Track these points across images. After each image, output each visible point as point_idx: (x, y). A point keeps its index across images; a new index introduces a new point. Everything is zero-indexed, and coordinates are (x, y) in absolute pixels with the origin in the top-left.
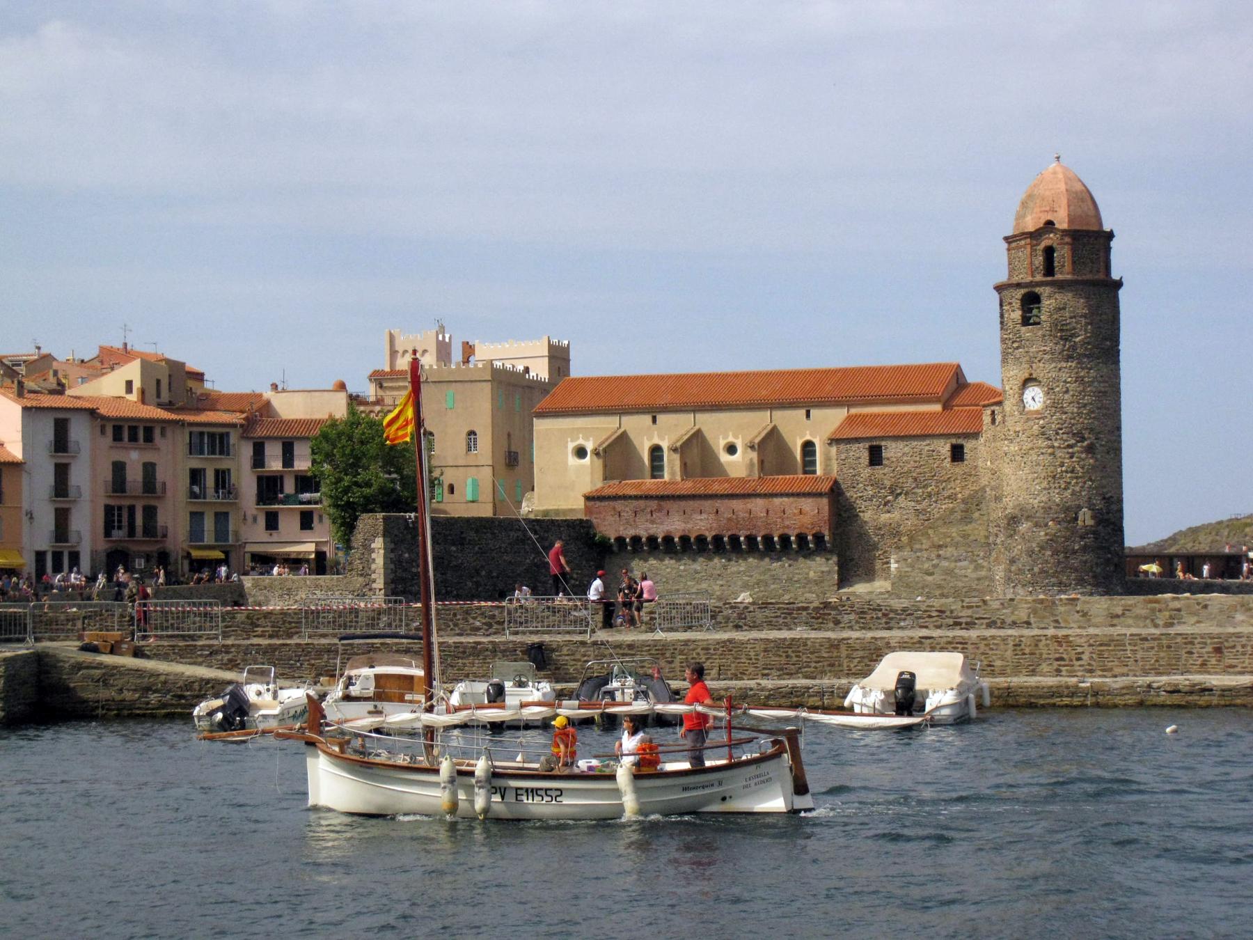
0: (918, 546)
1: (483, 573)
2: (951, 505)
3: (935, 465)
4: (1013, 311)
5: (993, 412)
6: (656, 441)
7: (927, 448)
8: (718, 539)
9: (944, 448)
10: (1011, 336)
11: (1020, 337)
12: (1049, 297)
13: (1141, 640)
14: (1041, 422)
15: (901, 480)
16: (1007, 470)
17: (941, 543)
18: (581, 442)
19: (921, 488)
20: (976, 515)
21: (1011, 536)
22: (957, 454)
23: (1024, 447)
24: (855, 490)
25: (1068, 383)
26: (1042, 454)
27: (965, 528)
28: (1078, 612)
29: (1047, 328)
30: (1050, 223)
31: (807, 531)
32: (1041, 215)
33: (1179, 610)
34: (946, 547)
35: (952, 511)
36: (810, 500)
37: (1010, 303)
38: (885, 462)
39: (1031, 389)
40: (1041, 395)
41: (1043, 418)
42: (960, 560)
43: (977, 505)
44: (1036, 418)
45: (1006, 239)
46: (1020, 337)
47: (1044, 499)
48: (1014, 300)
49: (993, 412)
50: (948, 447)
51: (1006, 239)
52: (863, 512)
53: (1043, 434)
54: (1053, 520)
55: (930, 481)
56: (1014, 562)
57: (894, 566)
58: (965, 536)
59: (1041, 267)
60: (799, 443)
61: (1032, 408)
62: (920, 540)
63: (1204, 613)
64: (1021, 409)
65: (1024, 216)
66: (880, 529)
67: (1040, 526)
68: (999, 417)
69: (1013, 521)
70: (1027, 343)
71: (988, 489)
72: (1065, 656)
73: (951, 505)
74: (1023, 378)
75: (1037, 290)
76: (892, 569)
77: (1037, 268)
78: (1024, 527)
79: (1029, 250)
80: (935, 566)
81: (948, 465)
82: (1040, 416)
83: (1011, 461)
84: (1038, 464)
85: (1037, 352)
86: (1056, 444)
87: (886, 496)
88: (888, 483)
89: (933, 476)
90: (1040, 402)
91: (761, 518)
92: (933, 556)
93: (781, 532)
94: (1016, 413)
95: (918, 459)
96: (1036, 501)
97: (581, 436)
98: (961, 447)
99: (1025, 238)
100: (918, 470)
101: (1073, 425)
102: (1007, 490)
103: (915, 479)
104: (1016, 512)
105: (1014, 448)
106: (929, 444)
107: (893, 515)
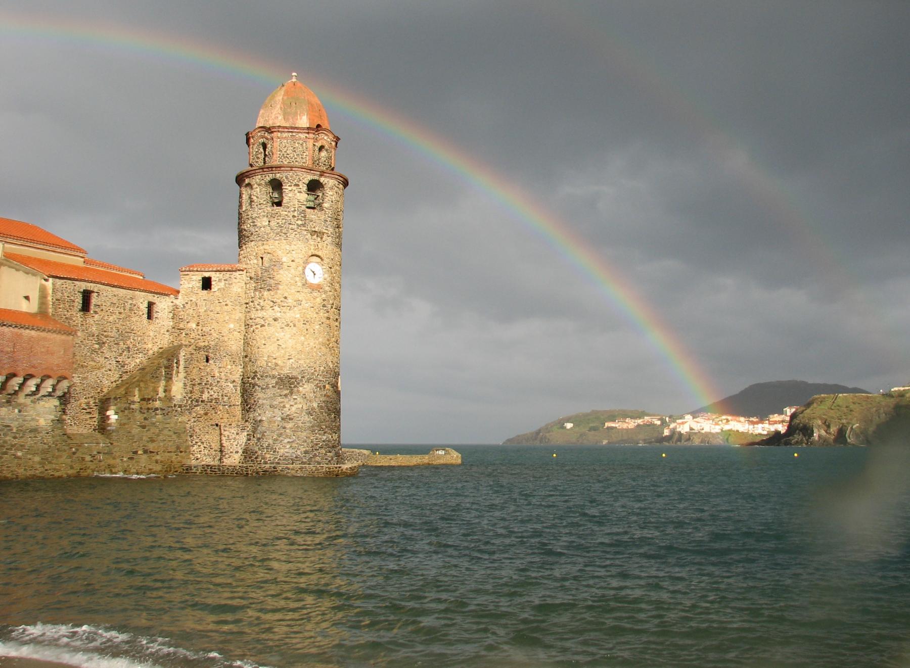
7: (130, 302)
9: (144, 307)
10: (296, 214)
12: (331, 188)
21: (286, 395)
29: (330, 215)
30: (319, 126)
37: (297, 185)
40: (321, 272)
46: (305, 217)
53: (324, 306)
54: (329, 384)
55: (130, 334)
57: (113, 416)
64: (304, 281)
68: (222, 284)
75: (322, 180)
79: (311, 143)
83: (288, 325)
89: (133, 330)
99: (308, 133)
104: (295, 374)
105: (295, 314)
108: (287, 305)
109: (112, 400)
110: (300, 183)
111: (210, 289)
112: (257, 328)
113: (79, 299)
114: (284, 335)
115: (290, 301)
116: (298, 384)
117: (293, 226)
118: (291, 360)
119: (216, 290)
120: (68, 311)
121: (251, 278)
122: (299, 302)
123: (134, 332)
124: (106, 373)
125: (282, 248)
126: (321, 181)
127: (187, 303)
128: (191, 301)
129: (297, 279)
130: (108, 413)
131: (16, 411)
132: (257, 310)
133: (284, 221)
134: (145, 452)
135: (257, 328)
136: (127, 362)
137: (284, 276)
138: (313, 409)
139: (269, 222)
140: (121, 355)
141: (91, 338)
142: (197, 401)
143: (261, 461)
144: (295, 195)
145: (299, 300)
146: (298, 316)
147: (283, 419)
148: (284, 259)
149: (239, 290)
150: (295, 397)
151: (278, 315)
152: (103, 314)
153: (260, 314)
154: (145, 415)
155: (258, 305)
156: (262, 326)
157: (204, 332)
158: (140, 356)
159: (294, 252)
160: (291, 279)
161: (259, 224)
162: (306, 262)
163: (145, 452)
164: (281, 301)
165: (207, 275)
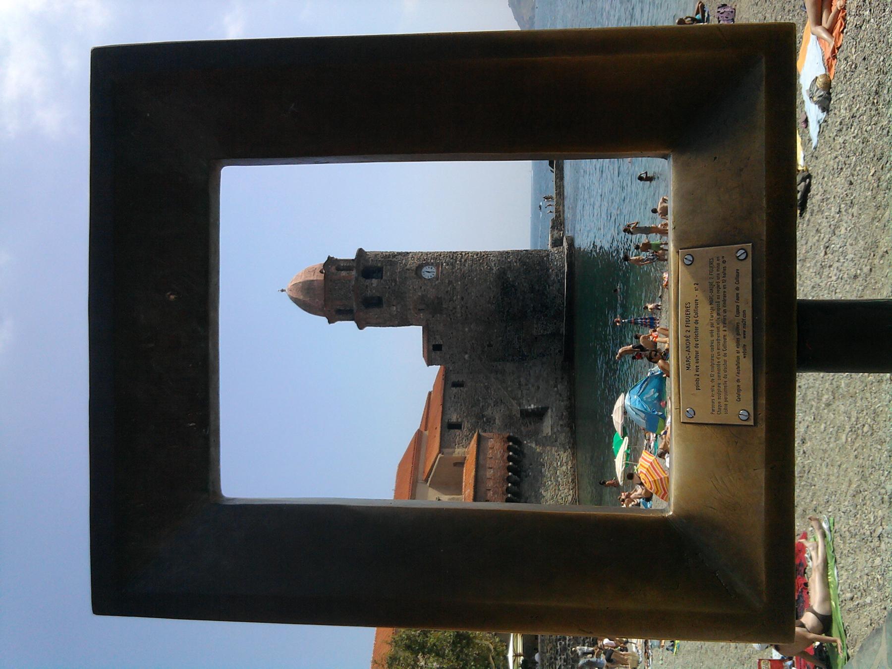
0: (519, 396)
3: (465, 395)
4: (372, 284)
7: (452, 399)
9: (455, 390)
10: (387, 287)
15: (473, 414)
19: (479, 404)
20: (500, 367)
21: (516, 290)
22: (456, 385)
23: (459, 275)
30: (321, 272)
31: (506, 445)
32: (315, 276)
34: (520, 381)
38: (460, 420)
39: (423, 274)
40: (427, 267)
41: (442, 264)
42: (530, 374)
44: (442, 267)
50: (454, 388)
56: (532, 287)
57: (532, 406)
59: (348, 272)
61: (435, 274)
66: (506, 425)
68: (437, 337)
70: (394, 276)
74: (415, 276)
76: (535, 407)
80: (533, 386)
81: (466, 389)
82: (440, 267)
83: (466, 290)
84: (472, 266)
85: (400, 266)
86: (460, 258)
90: (431, 268)
91: (494, 473)
93: (506, 461)
94: (437, 282)
95: (459, 404)
96: (494, 268)
100: (467, 404)
103: (472, 407)
106: (451, 398)
107: (497, 418)
108: (452, 292)
109: (522, 408)
111: (441, 345)
112: (469, 312)
113: (452, 431)
114: (473, 292)
115: (449, 289)
116: (507, 282)
118: (491, 287)
119: (441, 341)
120: (463, 438)
121: (433, 317)
122: (450, 283)
123: (473, 396)
125: (411, 295)
126: (362, 269)
127: (451, 361)
128: (449, 358)
129: (434, 284)
130: (530, 411)
131: (531, 466)
132: (456, 312)
133: (393, 295)
134: (556, 386)
135: (469, 312)
137: (432, 294)
139: (394, 306)
140: (489, 405)
141: (480, 424)
142: (519, 352)
143: (562, 307)
144: (374, 287)
145: (449, 283)
146: (459, 283)
147: (532, 293)
148: (420, 294)
149: (442, 325)
150: (517, 284)
151: (459, 297)
153: (458, 309)
154: (530, 386)
155: (452, 311)
156: (467, 307)
157: (471, 348)
158: (490, 391)
159: (415, 287)
160: (433, 288)
161: (395, 313)
162: (421, 277)
163: (556, 386)
164: (450, 295)
165: (431, 348)
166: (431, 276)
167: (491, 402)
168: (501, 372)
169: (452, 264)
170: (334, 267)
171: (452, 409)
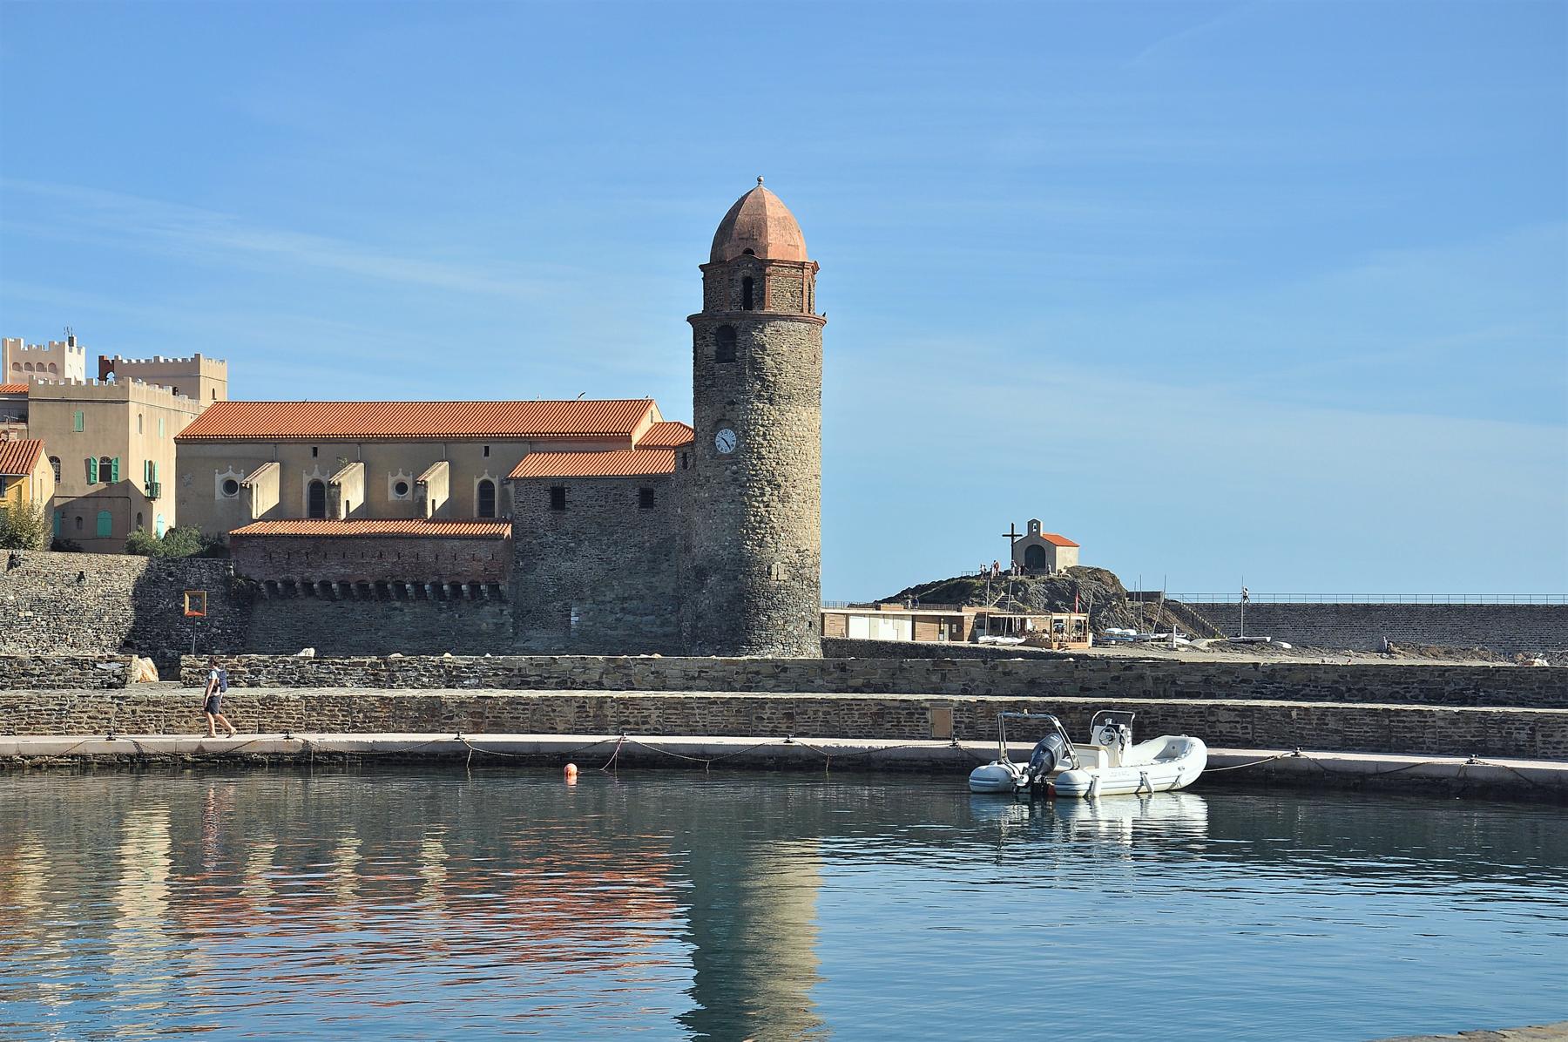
1: (106, 619)
2: (638, 554)
5: (685, 454)
6: (316, 475)
7: (614, 491)
8: (381, 585)
9: (633, 494)
11: (713, 375)
13: (710, 703)
14: (735, 468)
16: (697, 519)
17: (626, 595)
18: (231, 475)
20: (665, 565)
24: (535, 535)
25: (762, 426)
26: (733, 501)
27: (654, 580)
28: (652, 673)
31: (480, 580)
33: (757, 673)
34: (631, 600)
35: (639, 561)
36: (484, 544)
38: (567, 506)
42: (646, 615)
43: (665, 555)
45: (702, 267)
46: (713, 375)
47: (735, 551)
48: (707, 335)
49: (685, 454)
51: (702, 267)
52: (543, 559)
53: (736, 480)
57: (574, 619)
58: (651, 588)
60: (477, 482)
61: (724, 452)
62: (603, 592)
63: (782, 675)
65: (722, 243)
67: (730, 580)
69: (701, 574)
71: (677, 538)
72: (631, 720)
73: (638, 554)
77: (734, 300)
78: (712, 580)
87: (568, 543)
88: (571, 529)
89: (621, 522)
92: (618, 610)
97: (230, 467)
98: (652, 492)
100: (603, 515)
101: (768, 471)
102: (695, 541)
103: (599, 524)
104: (705, 563)
110: (707, 335)
113: (548, 496)
117: (703, 388)
120: (534, 512)
122: (707, 479)
124: (584, 572)
131: (457, 616)
136: (614, 559)
137: (699, 449)
138: (721, 607)
152: (577, 509)
166: (719, 446)
167: (609, 553)
168: (653, 568)
169: (736, 480)
170: (747, 273)
171: (591, 492)
